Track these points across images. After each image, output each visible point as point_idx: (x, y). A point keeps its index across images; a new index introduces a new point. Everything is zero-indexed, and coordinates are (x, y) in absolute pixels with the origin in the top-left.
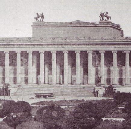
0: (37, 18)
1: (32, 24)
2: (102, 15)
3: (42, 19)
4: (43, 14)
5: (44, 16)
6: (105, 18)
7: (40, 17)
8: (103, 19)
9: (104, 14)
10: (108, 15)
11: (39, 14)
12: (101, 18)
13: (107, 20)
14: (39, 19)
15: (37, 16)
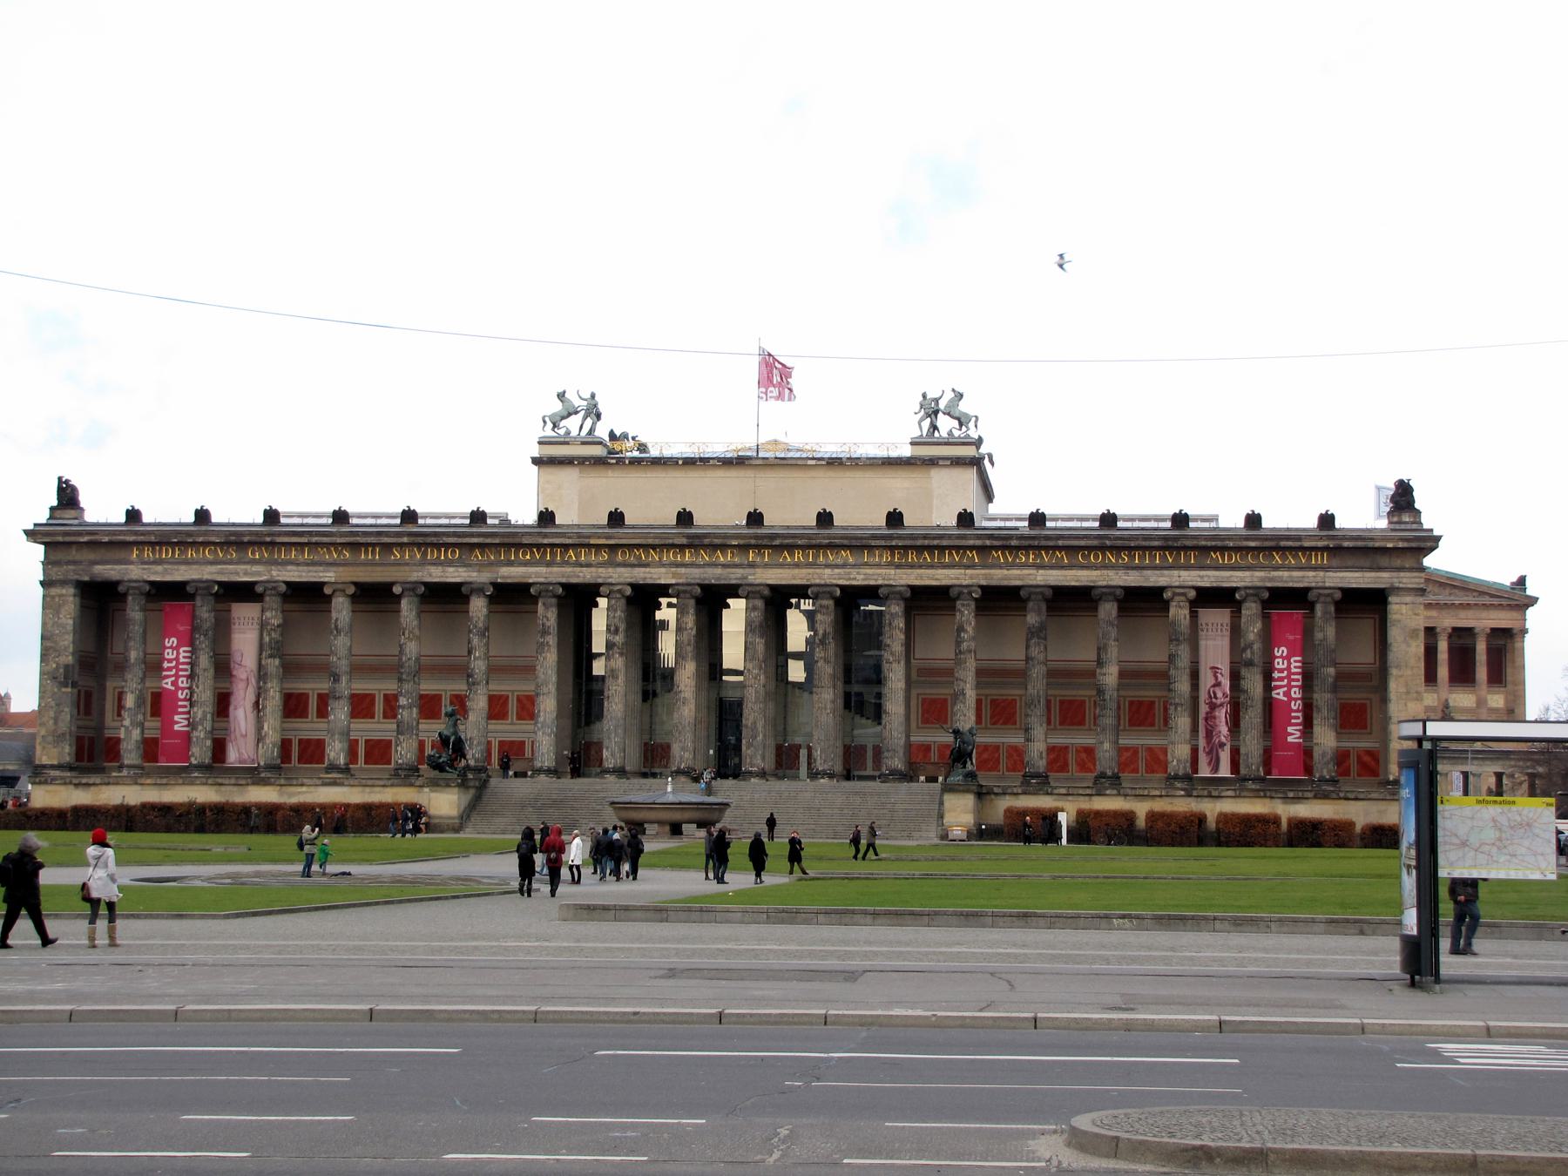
0: (563, 418)
1: (536, 451)
2: (931, 410)
3: (589, 422)
4: (593, 396)
5: (601, 407)
6: (945, 424)
7: (576, 413)
8: (934, 427)
9: (942, 404)
10: (964, 407)
11: (570, 396)
12: (926, 423)
13: (956, 433)
14: (573, 424)
15: (557, 407)
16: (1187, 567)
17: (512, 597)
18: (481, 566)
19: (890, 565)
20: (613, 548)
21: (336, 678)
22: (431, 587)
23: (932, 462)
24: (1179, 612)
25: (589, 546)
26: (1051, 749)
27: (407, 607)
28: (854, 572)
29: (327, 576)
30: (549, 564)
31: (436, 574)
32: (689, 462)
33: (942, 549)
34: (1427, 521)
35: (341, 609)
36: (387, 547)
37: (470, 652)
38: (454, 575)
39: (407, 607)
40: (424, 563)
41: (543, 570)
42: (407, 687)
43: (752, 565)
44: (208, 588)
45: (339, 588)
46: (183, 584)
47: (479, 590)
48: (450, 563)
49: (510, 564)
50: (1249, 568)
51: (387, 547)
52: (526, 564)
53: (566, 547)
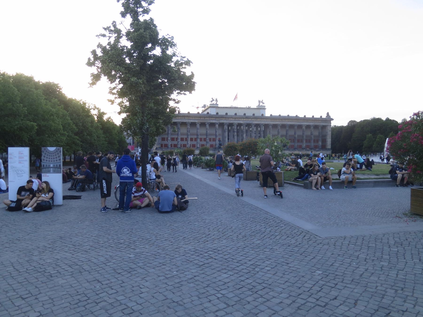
2: (259, 102)
8: (260, 104)
10: (263, 102)
15: (212, 100)
16: (305, 122)
17: (222, 125)
18: (218, 120)
19: (271, 121)
20: (235, 118)
21: (198, 136)
22: (211, 123)
23: (261, 109)
24: (304, 128)
25: (232, 118)
26: (297, 145)
27: (207, 126)
28: (266, 122)
29: (197, 121)
30: (227, 120)
31: (212, 121)
32: (230, 108)
33: (277, 119)
34: (331, 117)
35: (198, 126)
36: (205, 117)
37: (216, 132)
38: (214, 121)
39: (207, 126)
40: (210, 120)
41: (226, 121)
42: (208, 137)
43: (253, 121)
44: (180, 123)
45: (198, 123)
46: (176, 122)
47: (217, 124)
48: (213, 120)
49: (221, 120)
50: (312, 122)
51: (205, 117)
52: (224, 120)
53: (229, 118)
